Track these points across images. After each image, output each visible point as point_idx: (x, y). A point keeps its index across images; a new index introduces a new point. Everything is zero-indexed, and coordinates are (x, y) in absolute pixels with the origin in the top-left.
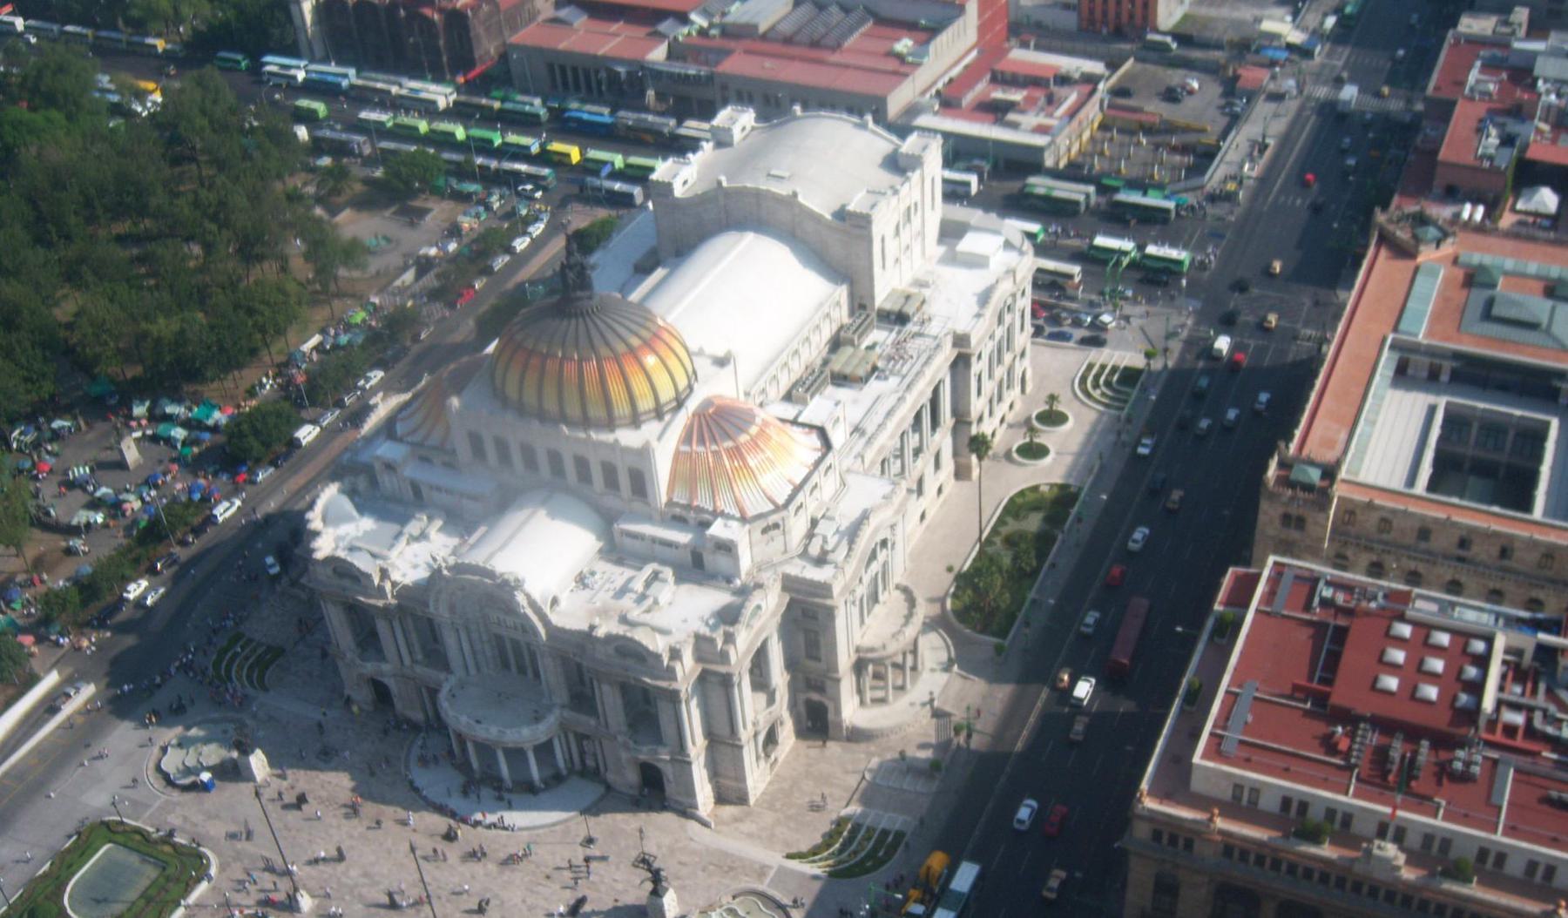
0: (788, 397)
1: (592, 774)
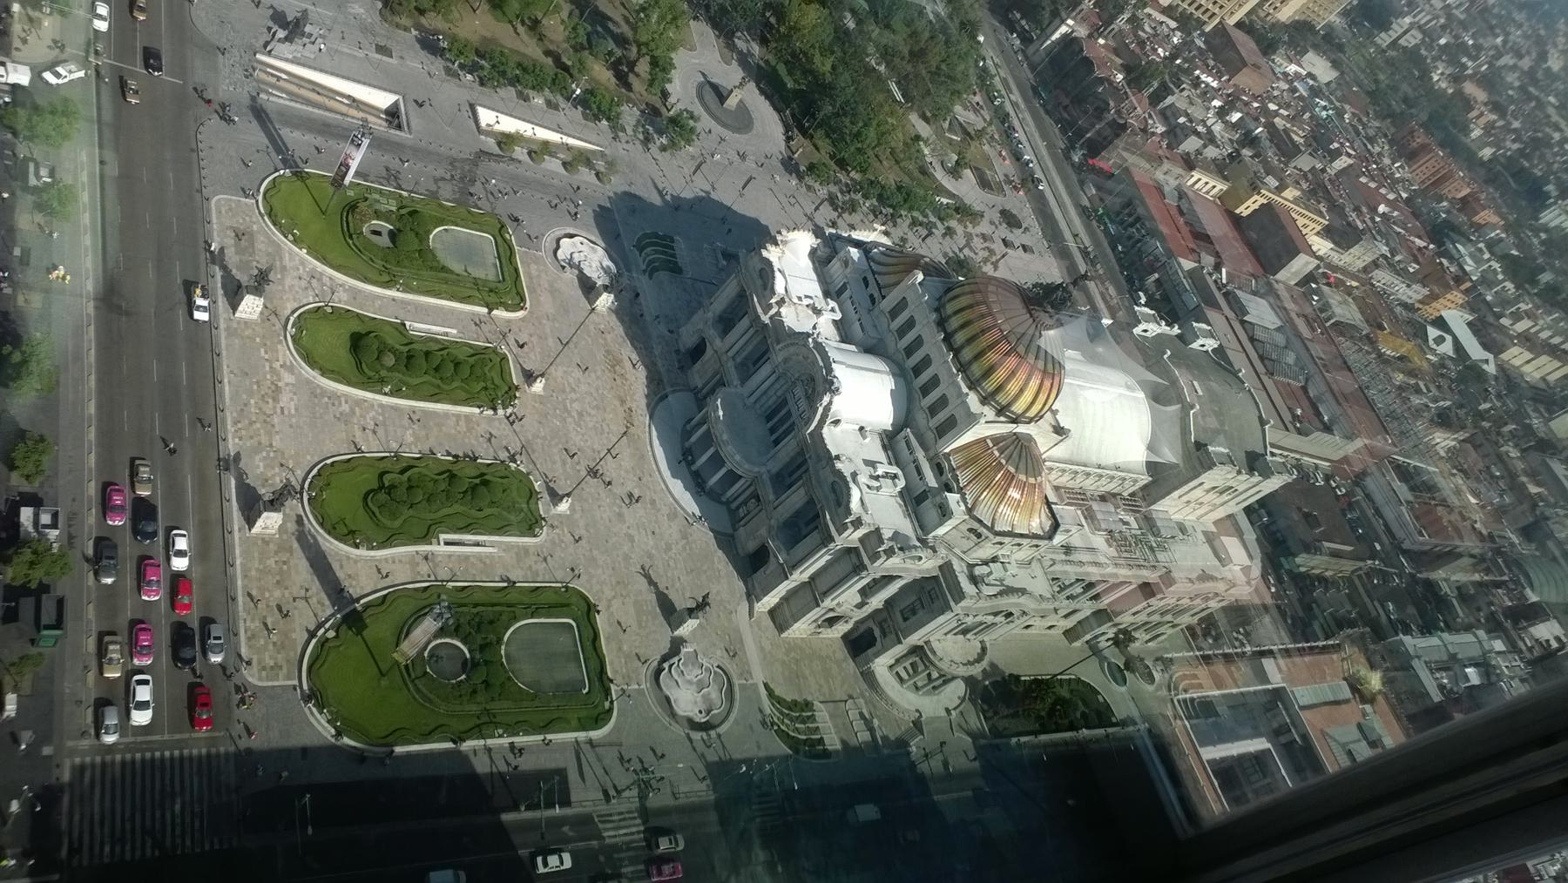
0: (1057, 488)
1: (735, 520)
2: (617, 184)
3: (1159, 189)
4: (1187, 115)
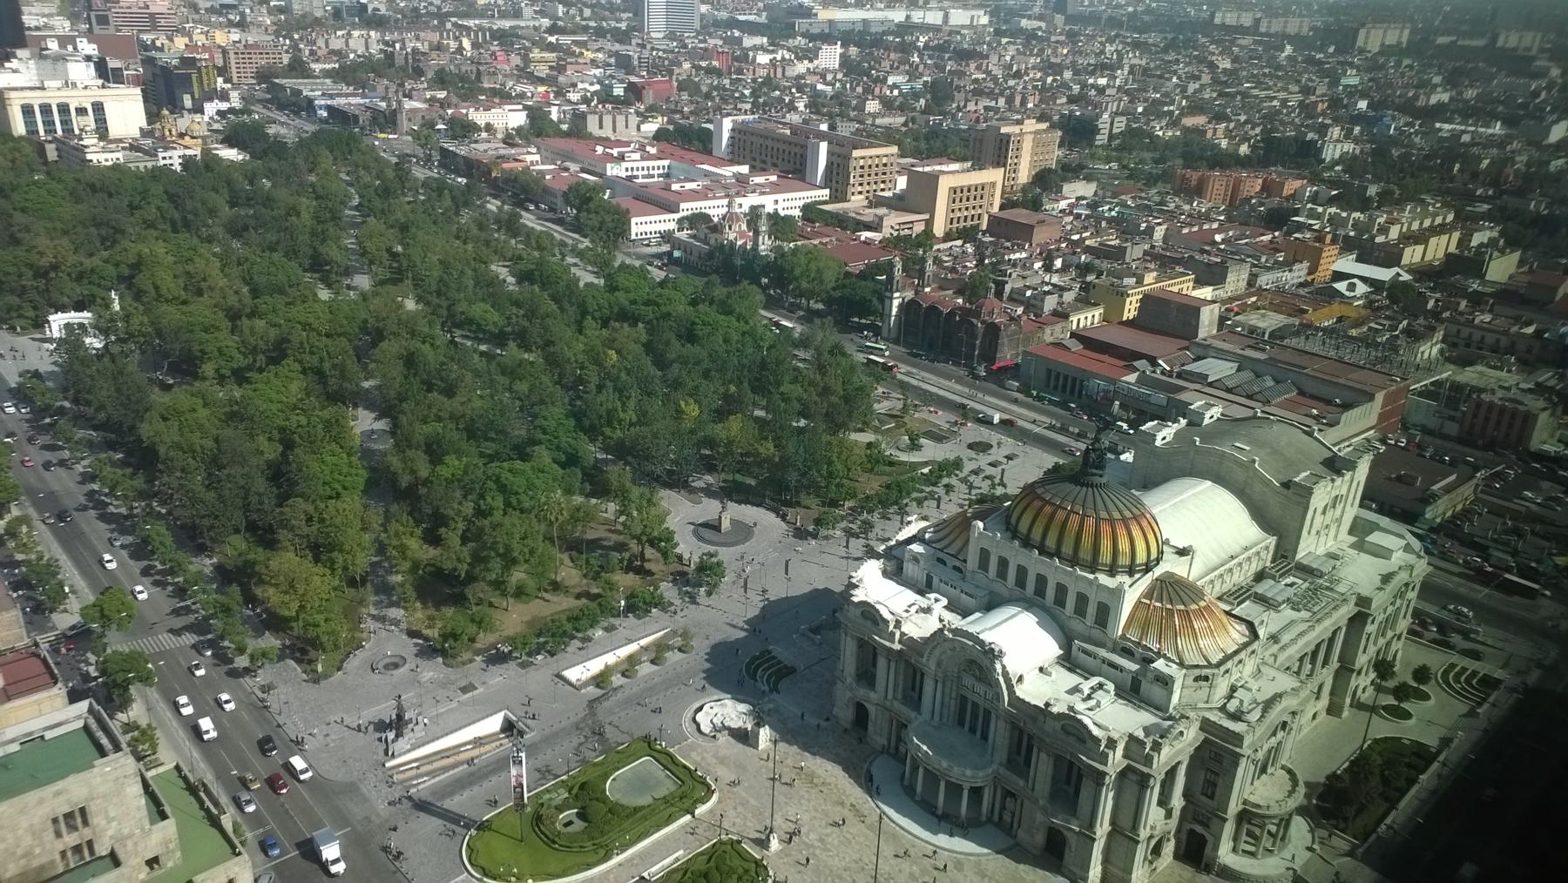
1: (1007, 829)
2: (701, 647)
3: (1059, 345)
4: (1029, 287)
